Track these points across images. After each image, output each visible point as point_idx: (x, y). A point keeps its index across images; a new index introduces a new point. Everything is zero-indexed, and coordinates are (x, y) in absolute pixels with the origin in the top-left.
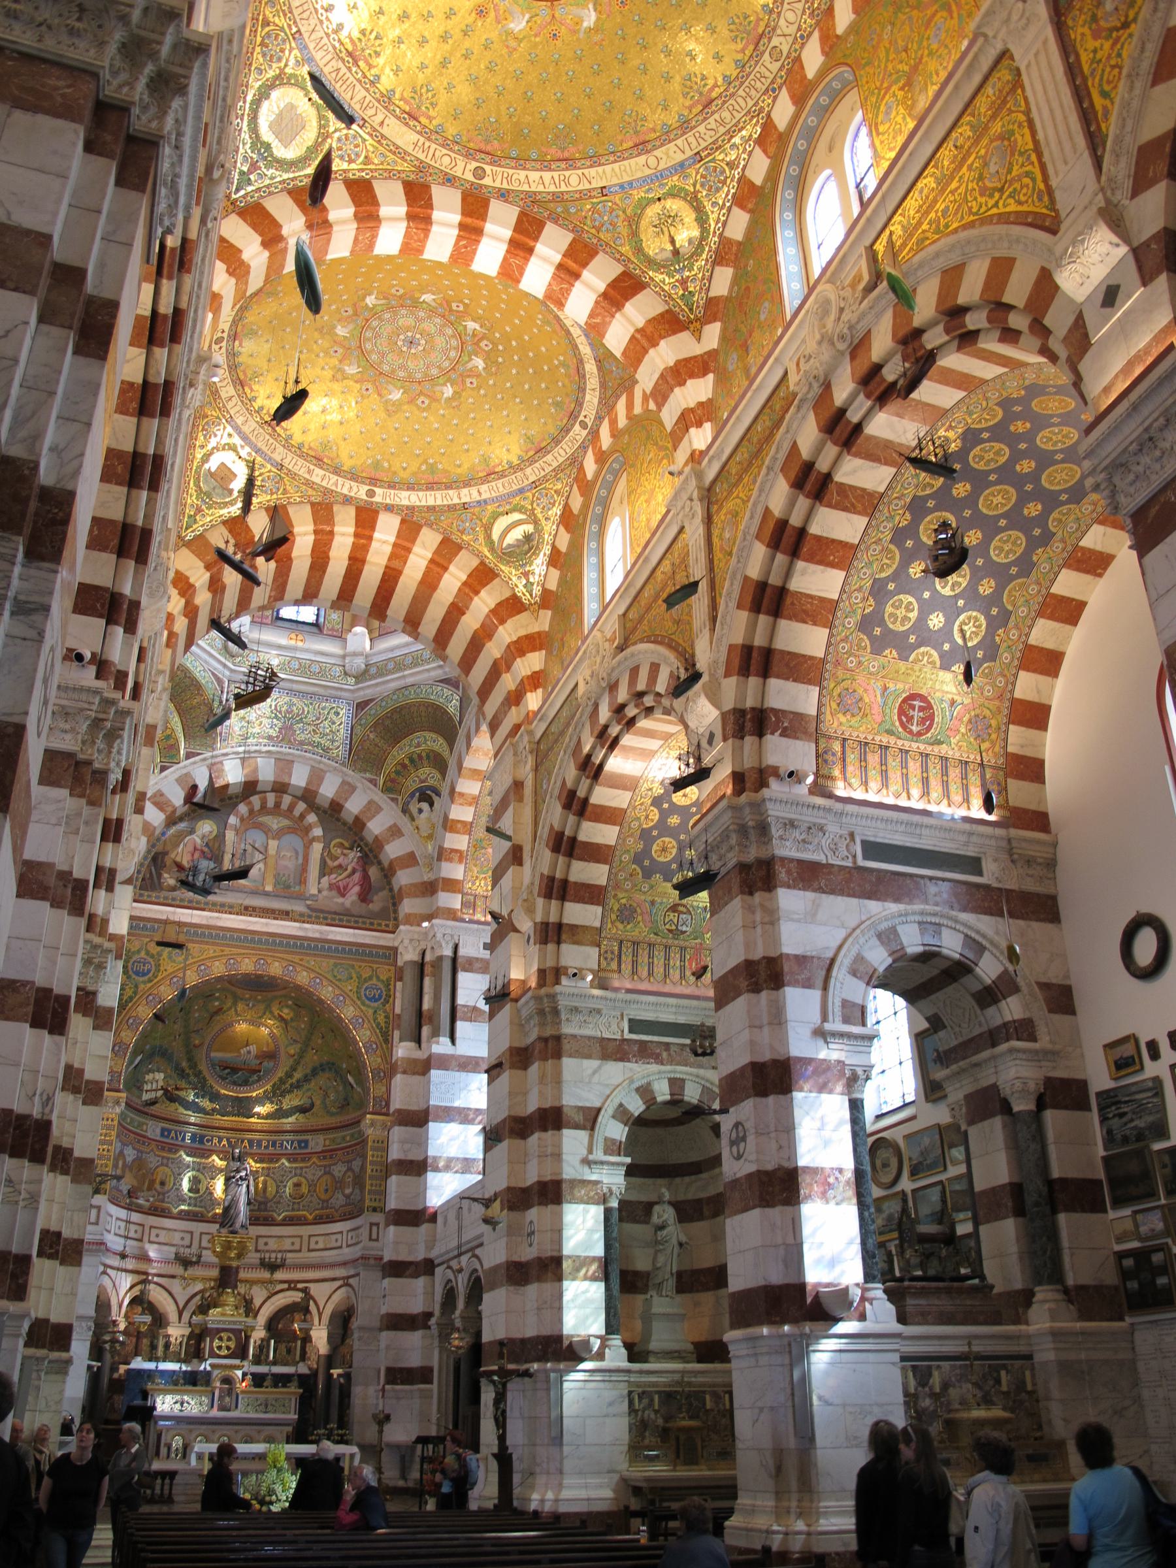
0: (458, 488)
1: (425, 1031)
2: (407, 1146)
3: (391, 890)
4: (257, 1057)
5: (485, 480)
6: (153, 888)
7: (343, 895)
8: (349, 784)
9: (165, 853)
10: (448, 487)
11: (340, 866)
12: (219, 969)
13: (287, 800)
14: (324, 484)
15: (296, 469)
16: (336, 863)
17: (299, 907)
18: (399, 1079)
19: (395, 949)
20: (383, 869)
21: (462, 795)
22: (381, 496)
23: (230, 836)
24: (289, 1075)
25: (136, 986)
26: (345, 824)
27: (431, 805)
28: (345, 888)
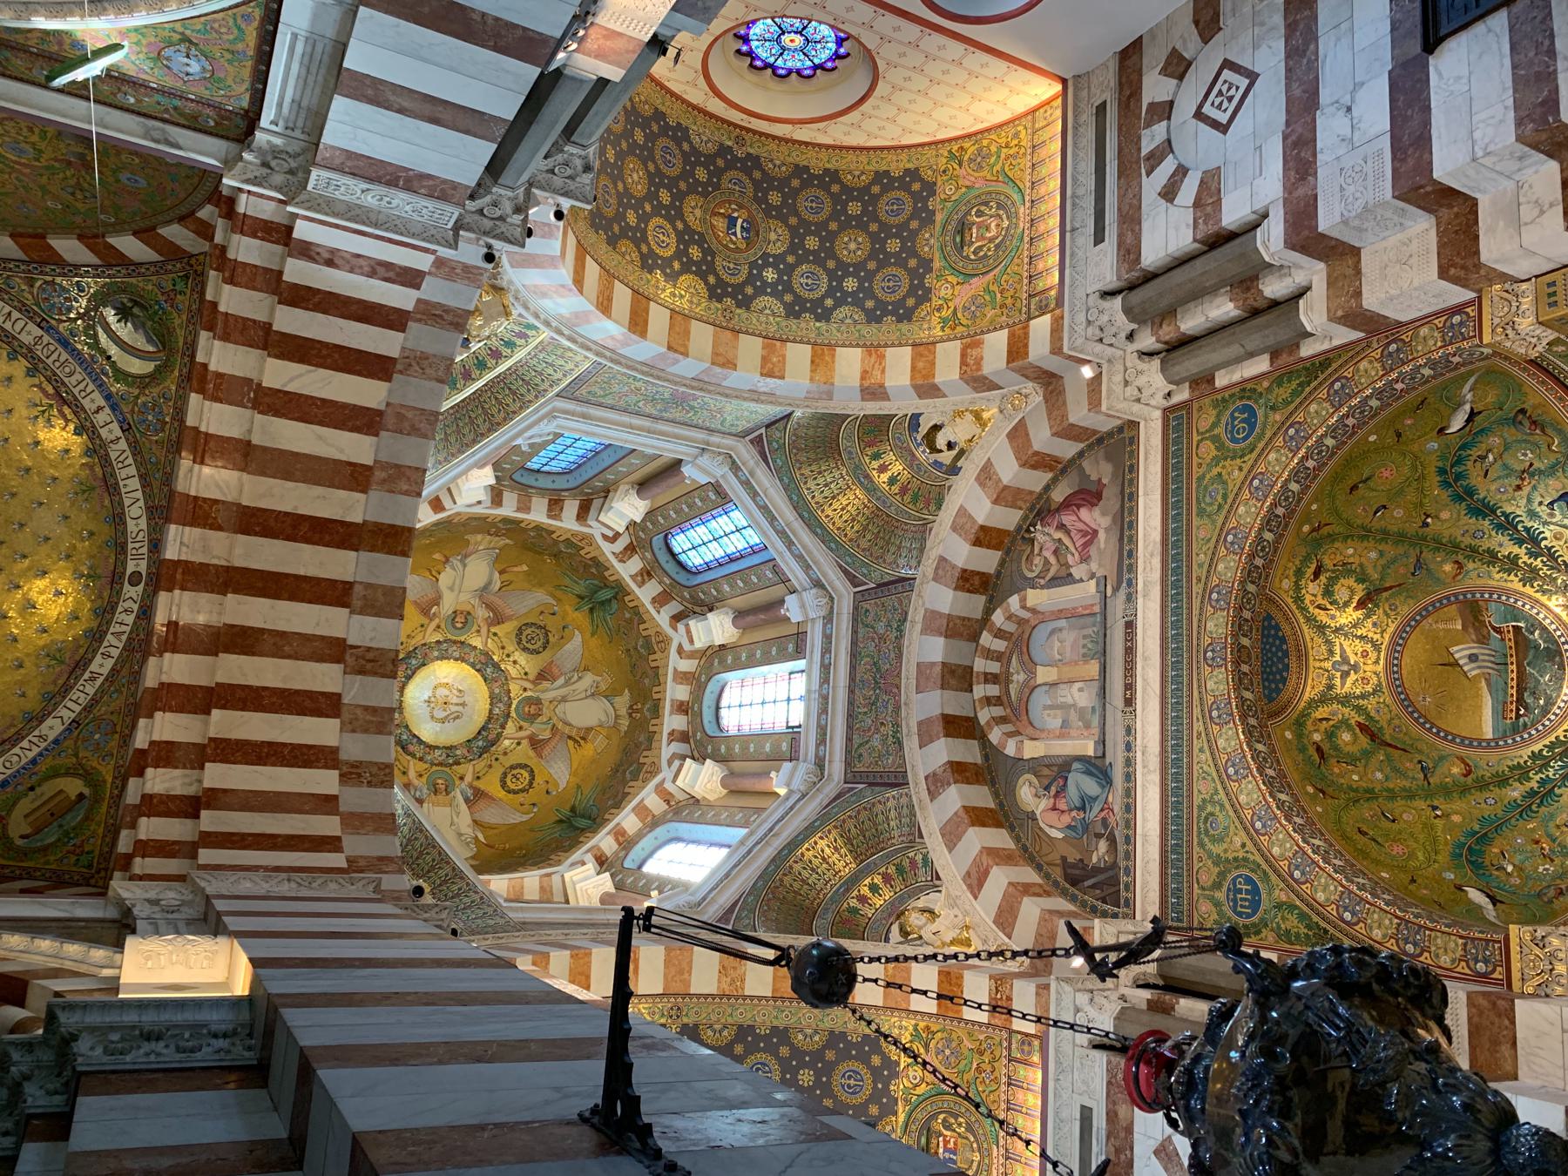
0: (104, 445)
1: (1273, 288)
2: (1527, 212)
3: (1081, 454)
4: (1483, 640)
5: (77, 408)
6: (1115, 881)
7: (1095, 532)
8: (937, 569)
9: (1064, 859)
10: (105, 461)
11: (1056, 552)
12: (1231, 738)
13: (980, 665)
14: (115, 653)
15: (83, 700)
16: (1052, 560)
17: (1118, 605)
18: (1373, 299)
19: (1166, 412)
20: (1055, 481)
21: (865, 374)
22: (137, 564)
23: (1032, 750)
24: (1511, 564)
25: (1279, 906)
26: (1002, 563)
27: (936, 428)
28: (1085, 534)
